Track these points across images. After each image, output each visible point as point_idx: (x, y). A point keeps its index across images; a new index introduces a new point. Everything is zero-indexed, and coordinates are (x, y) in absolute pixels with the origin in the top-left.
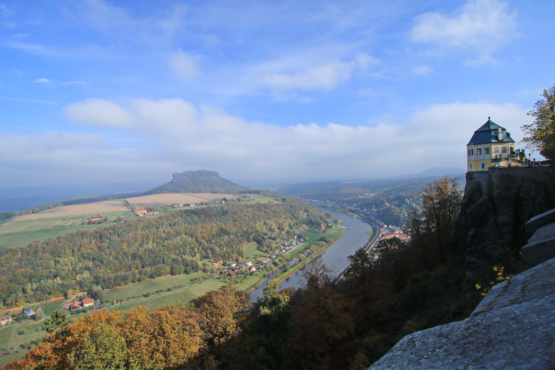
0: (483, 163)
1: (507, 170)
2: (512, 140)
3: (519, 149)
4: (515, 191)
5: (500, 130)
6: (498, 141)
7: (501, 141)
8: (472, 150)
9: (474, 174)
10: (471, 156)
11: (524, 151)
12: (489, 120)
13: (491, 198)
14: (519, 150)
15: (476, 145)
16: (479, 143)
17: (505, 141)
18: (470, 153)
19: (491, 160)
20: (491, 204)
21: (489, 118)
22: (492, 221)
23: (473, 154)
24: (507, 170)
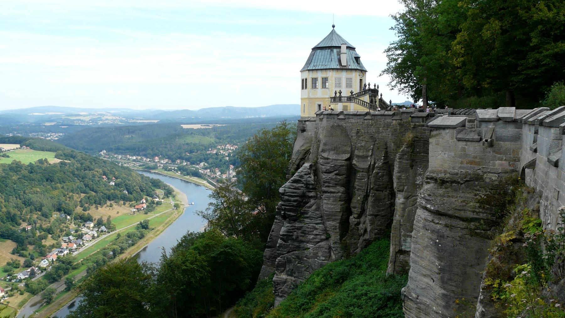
0: (319, 103)
1: (339, 117)
2: (363, 67)
3: (369, 83)
4: (348, 156)
5: (344, 49)
6: (341, 67)
7: (346, 68)
8: (306, 79)
9: (307, 123)
10: (304, 90)
11: (378, 87)
12: (332, 31)
13: (315, 169)
14: (369, 85)
15: (311, 72)
16: (314, 68)
17: (350, 67)
19: (330, 99)
21: (333, 26)
22: (314, 207)
23: (306, 88)
24: (339, 117)
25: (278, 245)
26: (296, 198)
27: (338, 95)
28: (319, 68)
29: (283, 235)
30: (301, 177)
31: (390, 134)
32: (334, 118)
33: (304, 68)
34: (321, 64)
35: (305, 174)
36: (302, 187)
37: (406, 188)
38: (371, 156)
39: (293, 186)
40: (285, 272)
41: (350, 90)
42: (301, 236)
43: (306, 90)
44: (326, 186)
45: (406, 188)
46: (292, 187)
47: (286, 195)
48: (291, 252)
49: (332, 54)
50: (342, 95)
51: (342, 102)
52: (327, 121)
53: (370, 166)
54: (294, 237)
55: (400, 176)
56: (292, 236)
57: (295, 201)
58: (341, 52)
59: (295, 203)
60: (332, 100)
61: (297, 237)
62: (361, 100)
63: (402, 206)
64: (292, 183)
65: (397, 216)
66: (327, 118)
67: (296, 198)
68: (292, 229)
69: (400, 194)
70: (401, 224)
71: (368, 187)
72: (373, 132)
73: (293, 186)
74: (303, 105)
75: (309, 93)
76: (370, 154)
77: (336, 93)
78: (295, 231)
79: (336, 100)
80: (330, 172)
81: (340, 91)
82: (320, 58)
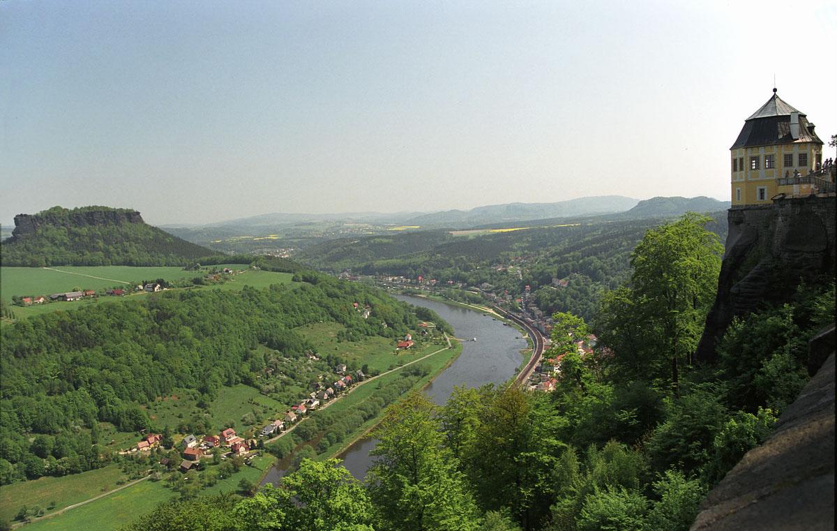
5: (795, 120)
10: (738, 173)
18: (737, 165)
21: (775, 90)
23: (741, 169)
74: (737, 191)
77: (787, 173)
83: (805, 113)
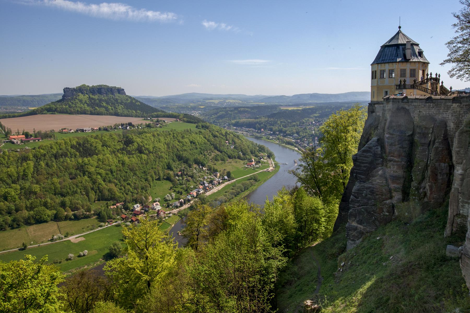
0: (386, 90)
8: (376, 71)
9: (376, 106)
10: (374, 80)
12: (399, 31)
14: (431, 74)
15: (380, 65)
16: (382, 62)
20: (380, 149)
21: (400, 27)
23: (375, 78)
25: (350, 200)
26: (365, 165)
27: (403, 83)
28: (387, 61)
29: (354, 193)
30: (370, 148)
31: (450, 115)
32: (399, 102)
33: (374, 62)
34: (388, 58)
35: (374, 146)
36: (371, 156)
37: (464, 161)
38: (432, 133)
39: (364, 155)
40: (356, 221)
41: (413, 79)
42: (369, 194)
43: (376, 80)
44: (392, 156)
45: (464, 161)
46: (363, 156)
47: (358, 162)
48: (361, 206)
49: (398, 50)
50: (407, 83)
51: (406, 89)
52: (393, 104)
53: (430, 142)
54: (363, 195)
55: (459, 151)
56: (363, 193)
57: (365, 167)
58: (406, 48)
59: (365, 169)
60: (398, 88)
61: (366, 195)
62: (423, 87)
63: (460, 177)
64: (363, 152)
65: (456, 185)
66: (393, 102)
67: (365, 165)
68: (363, 188)
69: (459, 166)
70: (459, 191)
71: (428, 159)
72: (434, 114)
73: (364, 155)
75: (378, 82)
76: (431, 132)
77: (401, 81)
78: (364, 190)
79: (401, 88)
80: (395, 146)
81: (405, 80)
82: (387, 54)
83: (418, 43)
